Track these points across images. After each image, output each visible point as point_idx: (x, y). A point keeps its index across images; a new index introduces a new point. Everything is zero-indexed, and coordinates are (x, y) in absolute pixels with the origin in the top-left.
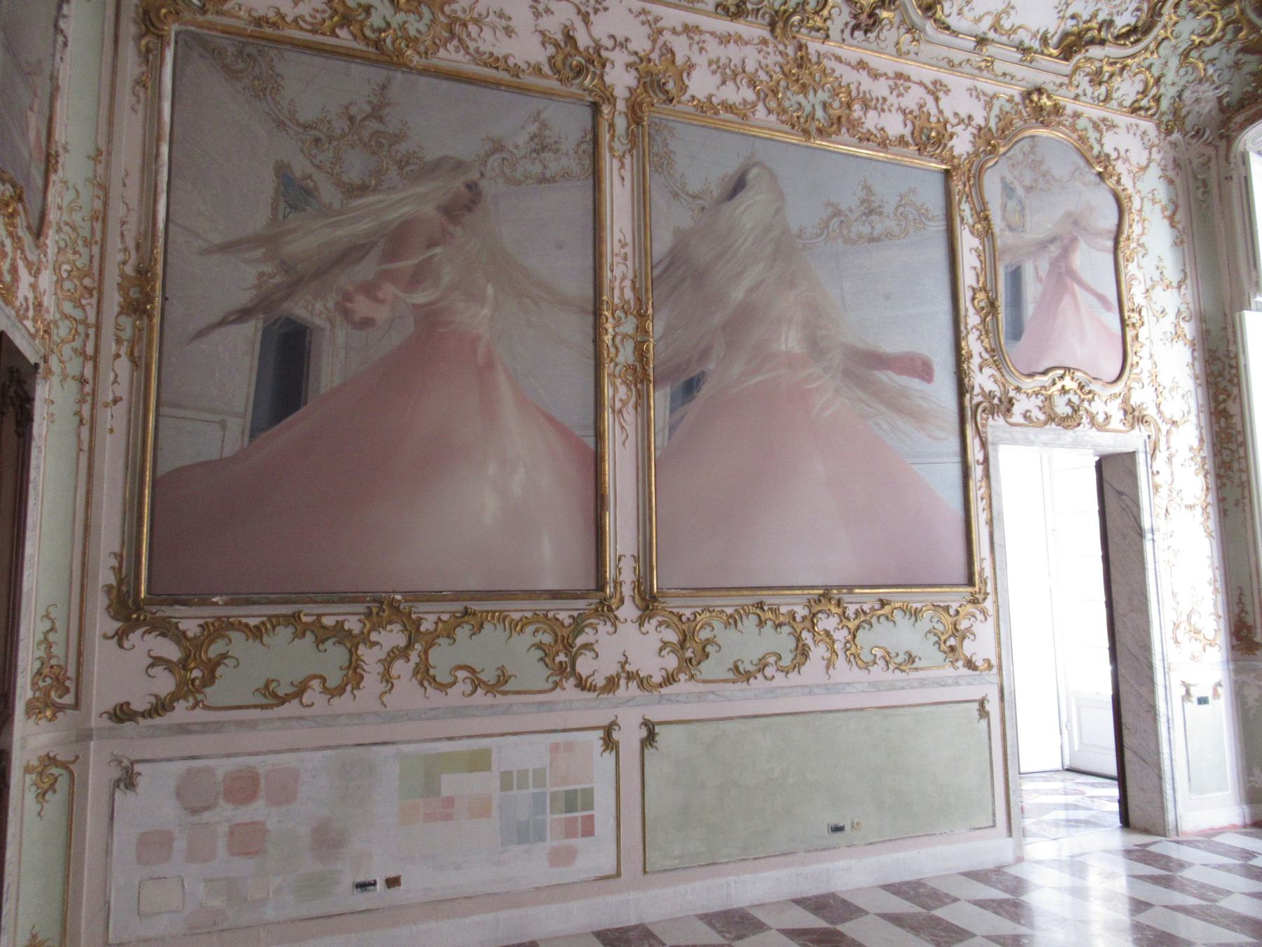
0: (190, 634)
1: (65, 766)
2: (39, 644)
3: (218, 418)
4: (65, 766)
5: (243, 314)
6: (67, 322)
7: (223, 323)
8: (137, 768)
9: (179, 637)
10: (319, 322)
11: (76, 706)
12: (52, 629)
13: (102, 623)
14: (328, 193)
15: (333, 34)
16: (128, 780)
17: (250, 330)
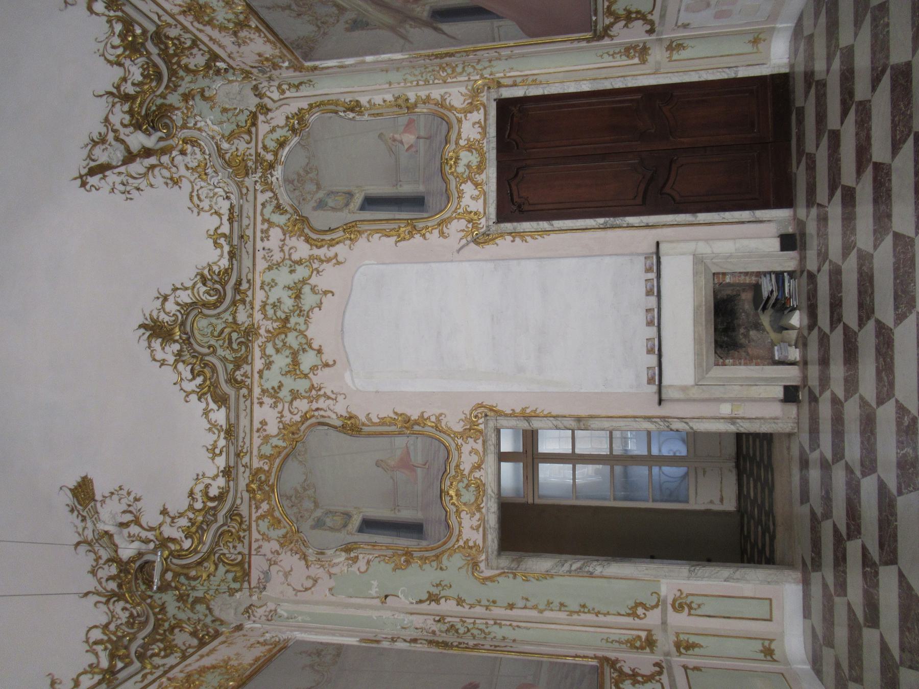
0: (612, 20)
1: (672, 42)
2: (614, 58)
3: (496, 30)
4: (672, 42)
5: (436, 29)
6: (466, 69)
7: (444, 33)
8: (680, 24)
9: (612, 25)
10: (427, 8)
11: (645, 43)
12: (607, 53)
13: (606, 41)
14: (350, 16)
15: (257, 27)
16: (685, 26)
17: (445, 27)
